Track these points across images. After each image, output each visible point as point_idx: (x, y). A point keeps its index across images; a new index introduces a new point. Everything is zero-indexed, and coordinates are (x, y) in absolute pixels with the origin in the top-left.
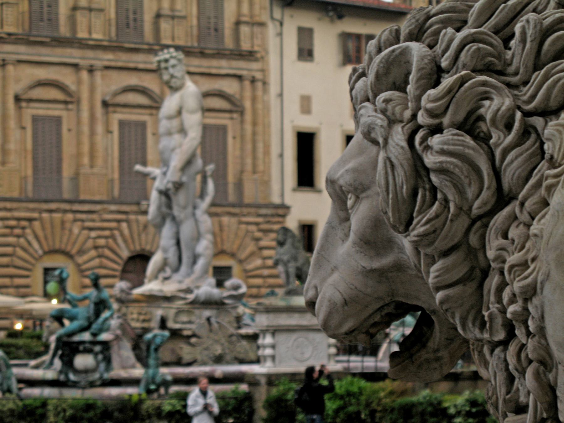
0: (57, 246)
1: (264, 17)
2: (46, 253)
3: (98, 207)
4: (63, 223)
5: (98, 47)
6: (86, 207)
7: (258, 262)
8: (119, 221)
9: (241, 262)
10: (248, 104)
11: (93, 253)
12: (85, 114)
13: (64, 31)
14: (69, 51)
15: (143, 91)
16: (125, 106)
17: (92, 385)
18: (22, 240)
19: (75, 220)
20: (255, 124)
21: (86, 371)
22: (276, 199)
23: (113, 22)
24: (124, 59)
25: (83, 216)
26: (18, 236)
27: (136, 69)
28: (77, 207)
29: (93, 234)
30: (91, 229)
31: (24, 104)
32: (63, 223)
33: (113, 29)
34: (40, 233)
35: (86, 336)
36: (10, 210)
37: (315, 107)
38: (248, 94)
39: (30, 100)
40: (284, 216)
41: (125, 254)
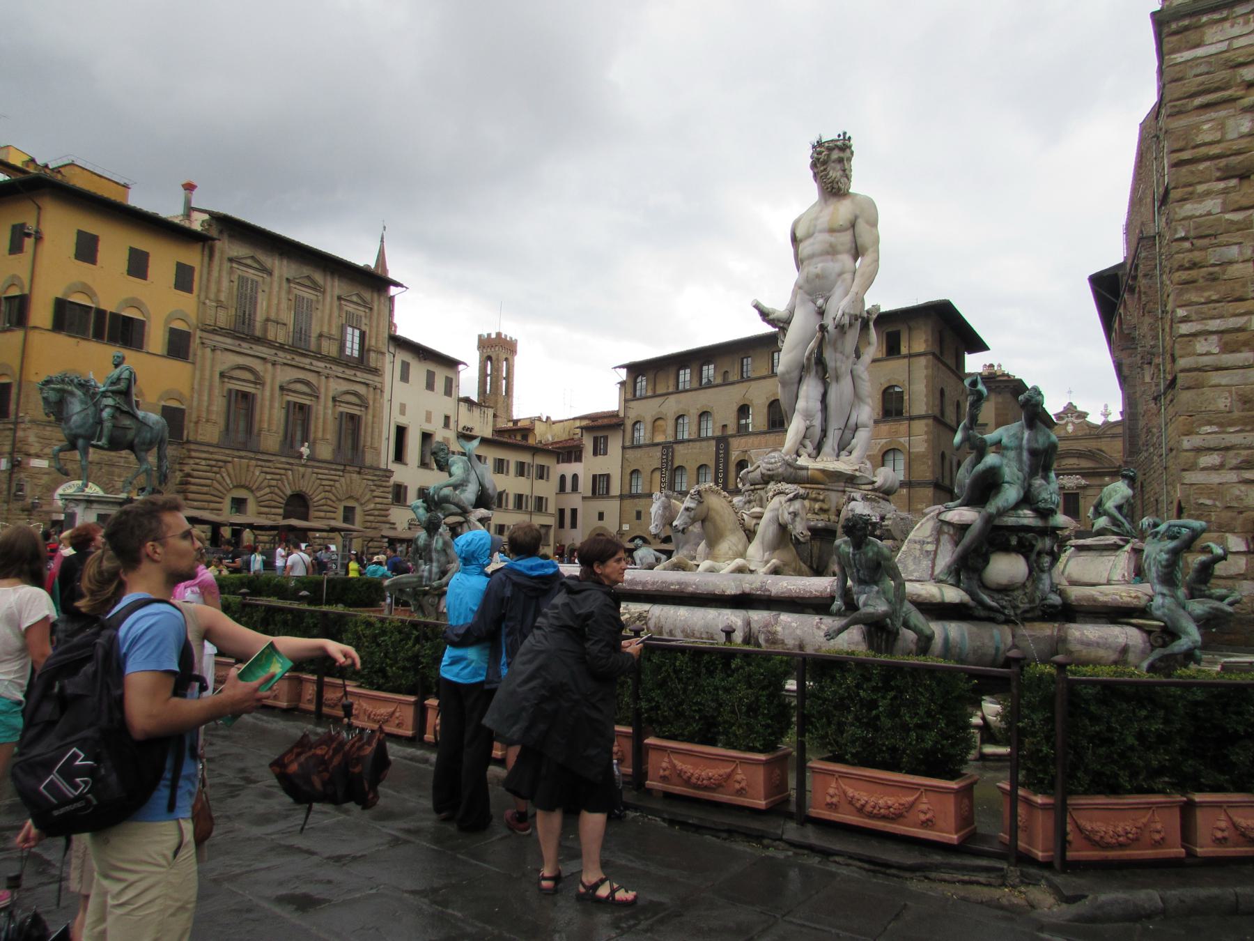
0: (243, 483)
1: (384, 349)
2: (235, 487)
3: (273, 458)
4: (248, 466)
5: (281, 347)
6: (265, 457)
7: (372, 506)
8: (286, 469)
9: (362, 504)
10: (371, 403)
11: (267, 490)
12: (268, 393)
13: (258, 333)
14: (260, 348)
15: (307, 383)
16: (294, 392)
17: (1029, 617)
18: (218, 476)
19: (257, 466)
20: (374, 416)
21: (1005, 590)
22: (383, 466)
23: (291, 334)
24: (299, 360)
25: (263, 463)
26: (216, 473)
27: (303, 369)
28: (260, 457)
29: (269, 477)
30: (267, 473)
31: (226, 380)
32: (248, 466)
33: (291, 340)
34: (231, 471)
35: (1027, 517)
36: (212, 453)
37: (407, 412)
38: (371, 397)
39: (232, 378)
40: (389, 477)
41: (289, 492)
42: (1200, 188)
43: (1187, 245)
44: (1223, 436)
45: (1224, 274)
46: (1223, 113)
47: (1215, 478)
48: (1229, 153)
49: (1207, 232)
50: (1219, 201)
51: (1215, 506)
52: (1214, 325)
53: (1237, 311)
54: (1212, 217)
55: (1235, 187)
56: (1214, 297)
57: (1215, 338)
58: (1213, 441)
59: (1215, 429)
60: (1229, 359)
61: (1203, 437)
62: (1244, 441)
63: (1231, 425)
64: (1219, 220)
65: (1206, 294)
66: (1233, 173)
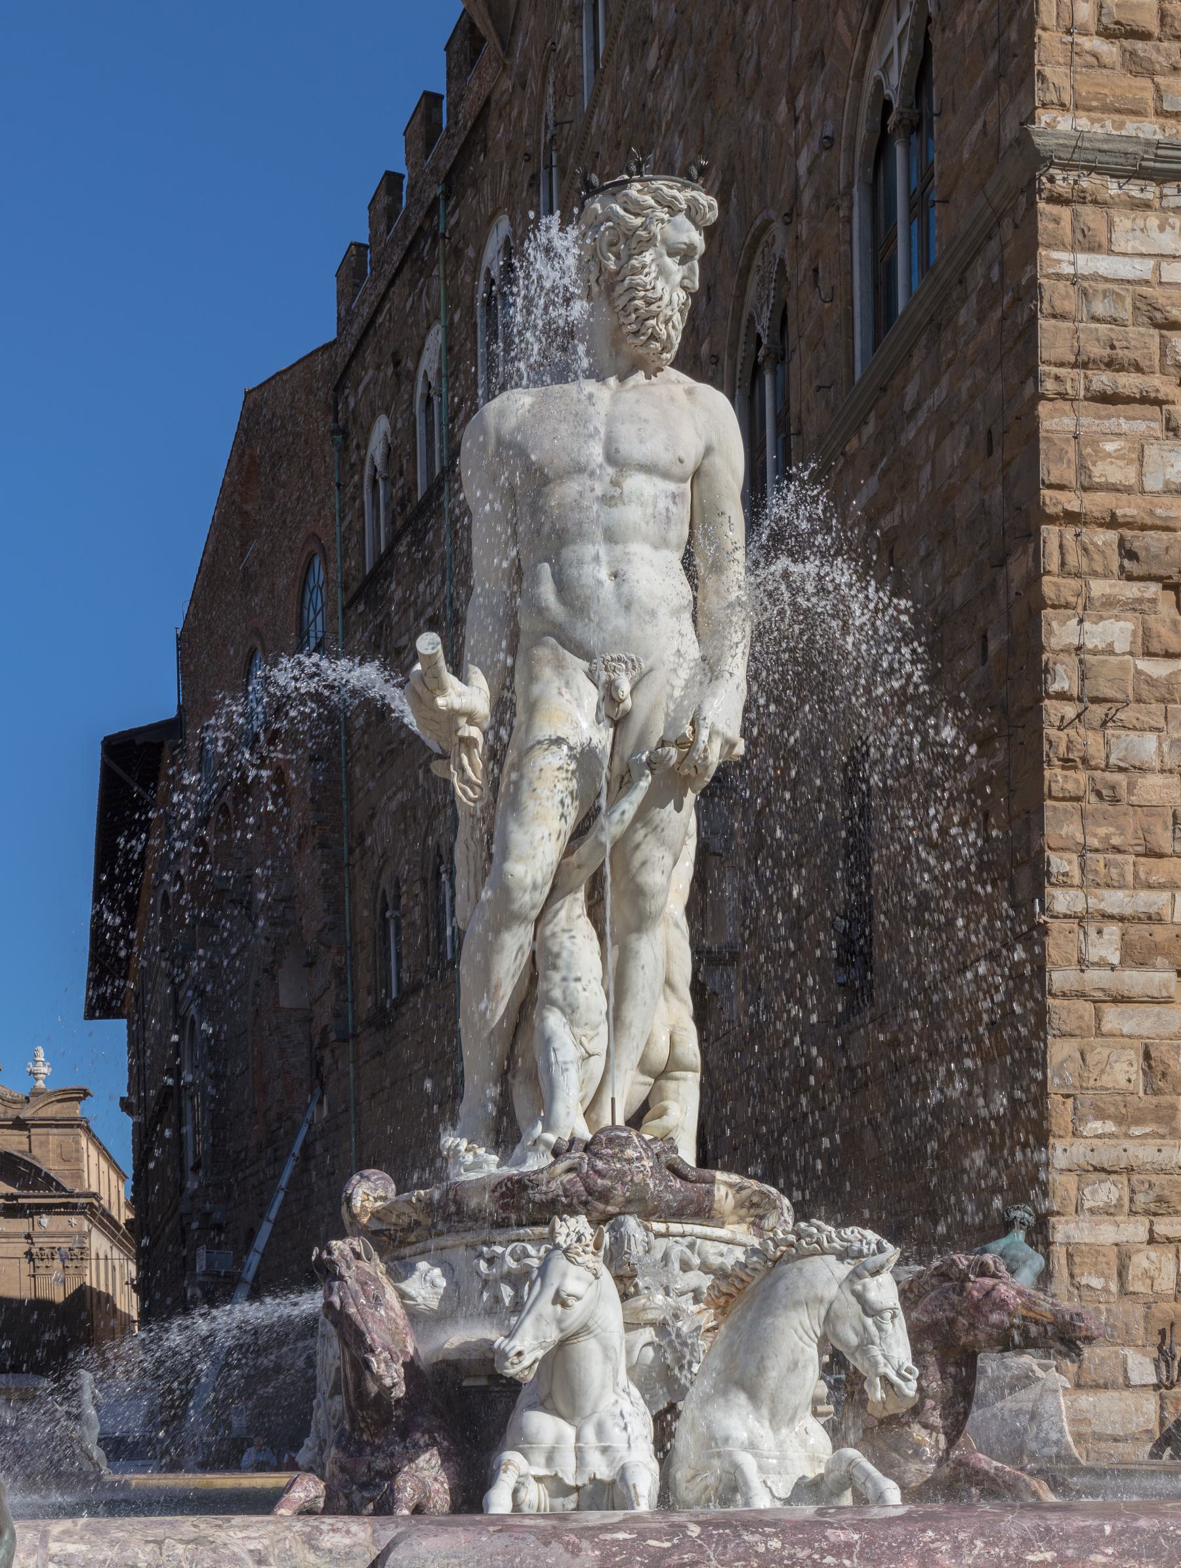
42: (1099, 588)
43: (1070, 711)
44: (1126, 1144)
45: (1130, 791)
46: (1141, 426)
47: (1107, 1233)
48: (1149, 521)
49: (1110, 693)
50: (1130, 626)
51: (1106, 1290)
52: (1115, 900)
53: (1153, 879)
54: (1112, 658)
55: (1153, 601)
56: (1115, 841)
57: (1113, 930)
58: (1107, 1155)
59: (1110, 1127)
60: (1135, 980)
61: (1088, 1141)
62: (1159, 1158)
63: (1138, 1121)
64: (1123, 668)
65: (1102, 831)
66: (1156, 570)
